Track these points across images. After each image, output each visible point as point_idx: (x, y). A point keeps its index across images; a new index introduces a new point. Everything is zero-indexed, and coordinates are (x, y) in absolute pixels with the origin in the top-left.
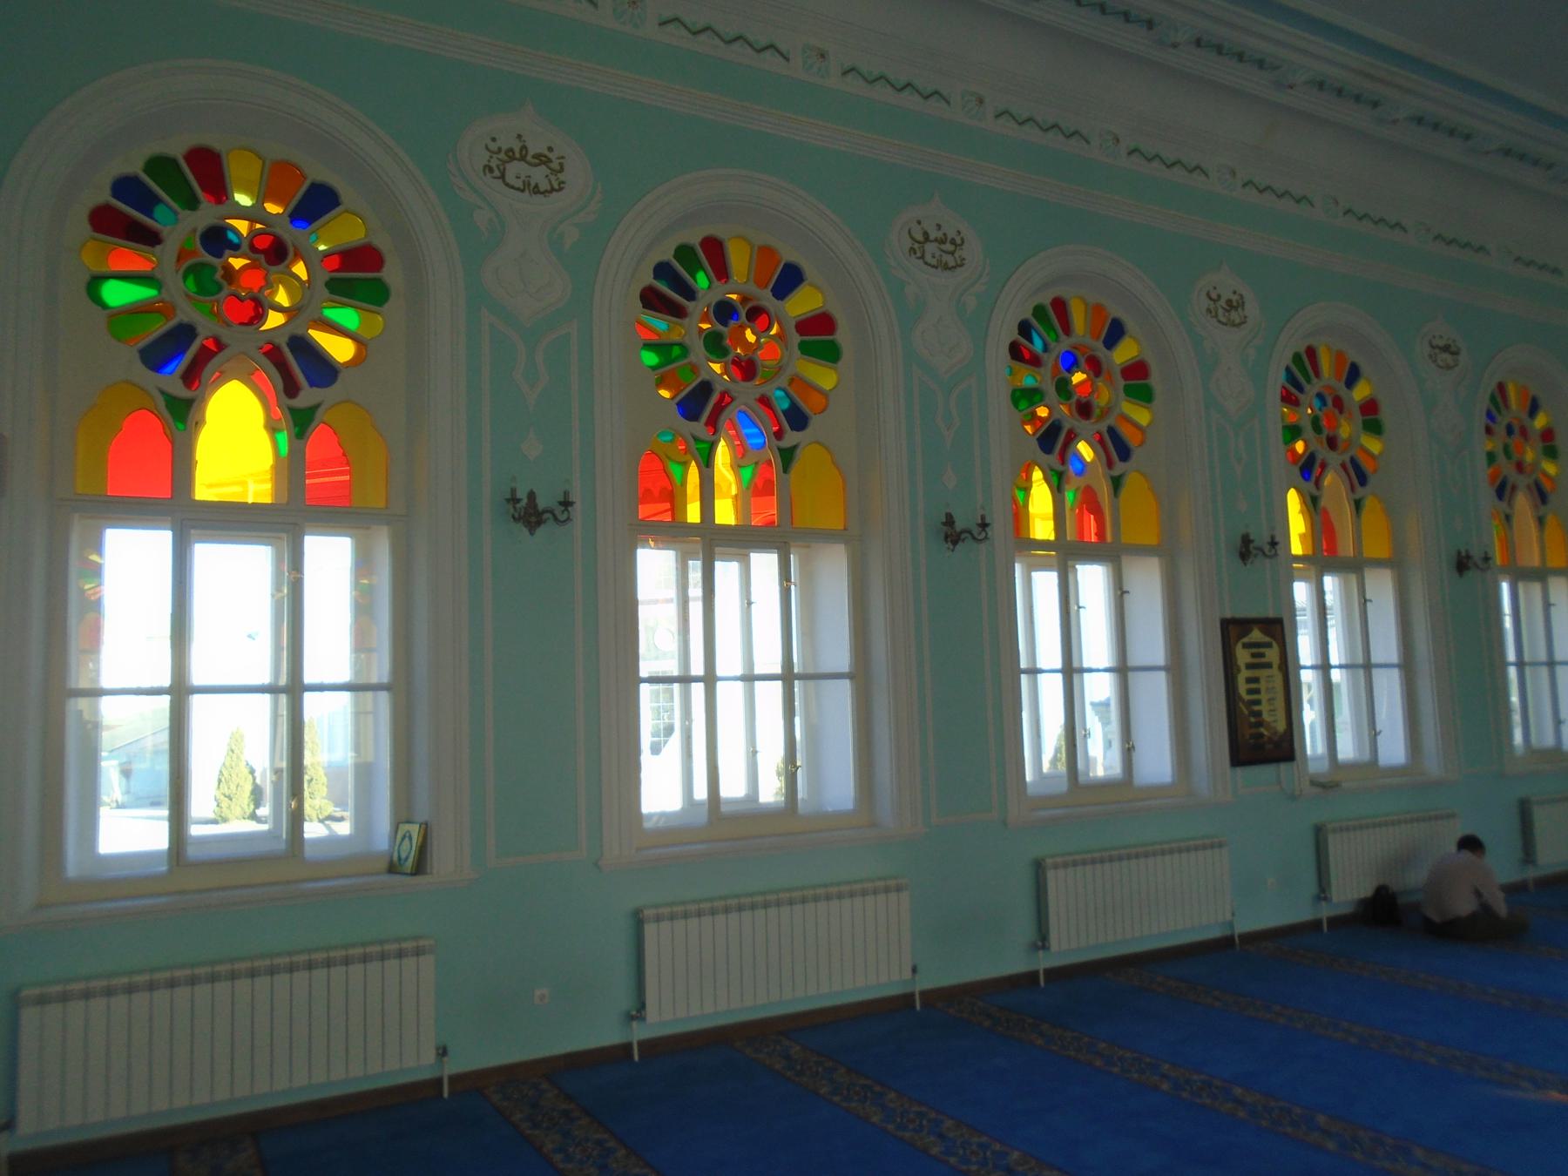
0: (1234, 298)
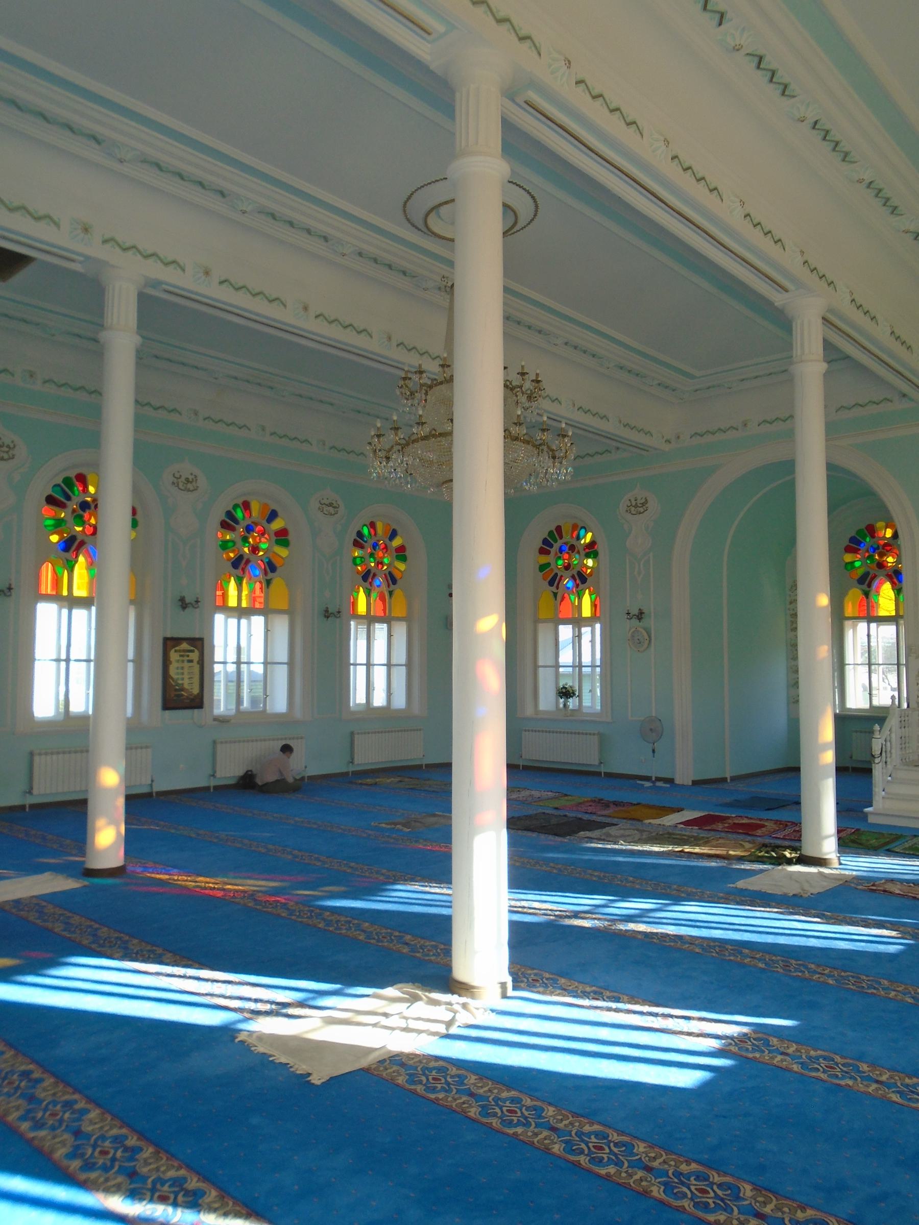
0: (190, 478)
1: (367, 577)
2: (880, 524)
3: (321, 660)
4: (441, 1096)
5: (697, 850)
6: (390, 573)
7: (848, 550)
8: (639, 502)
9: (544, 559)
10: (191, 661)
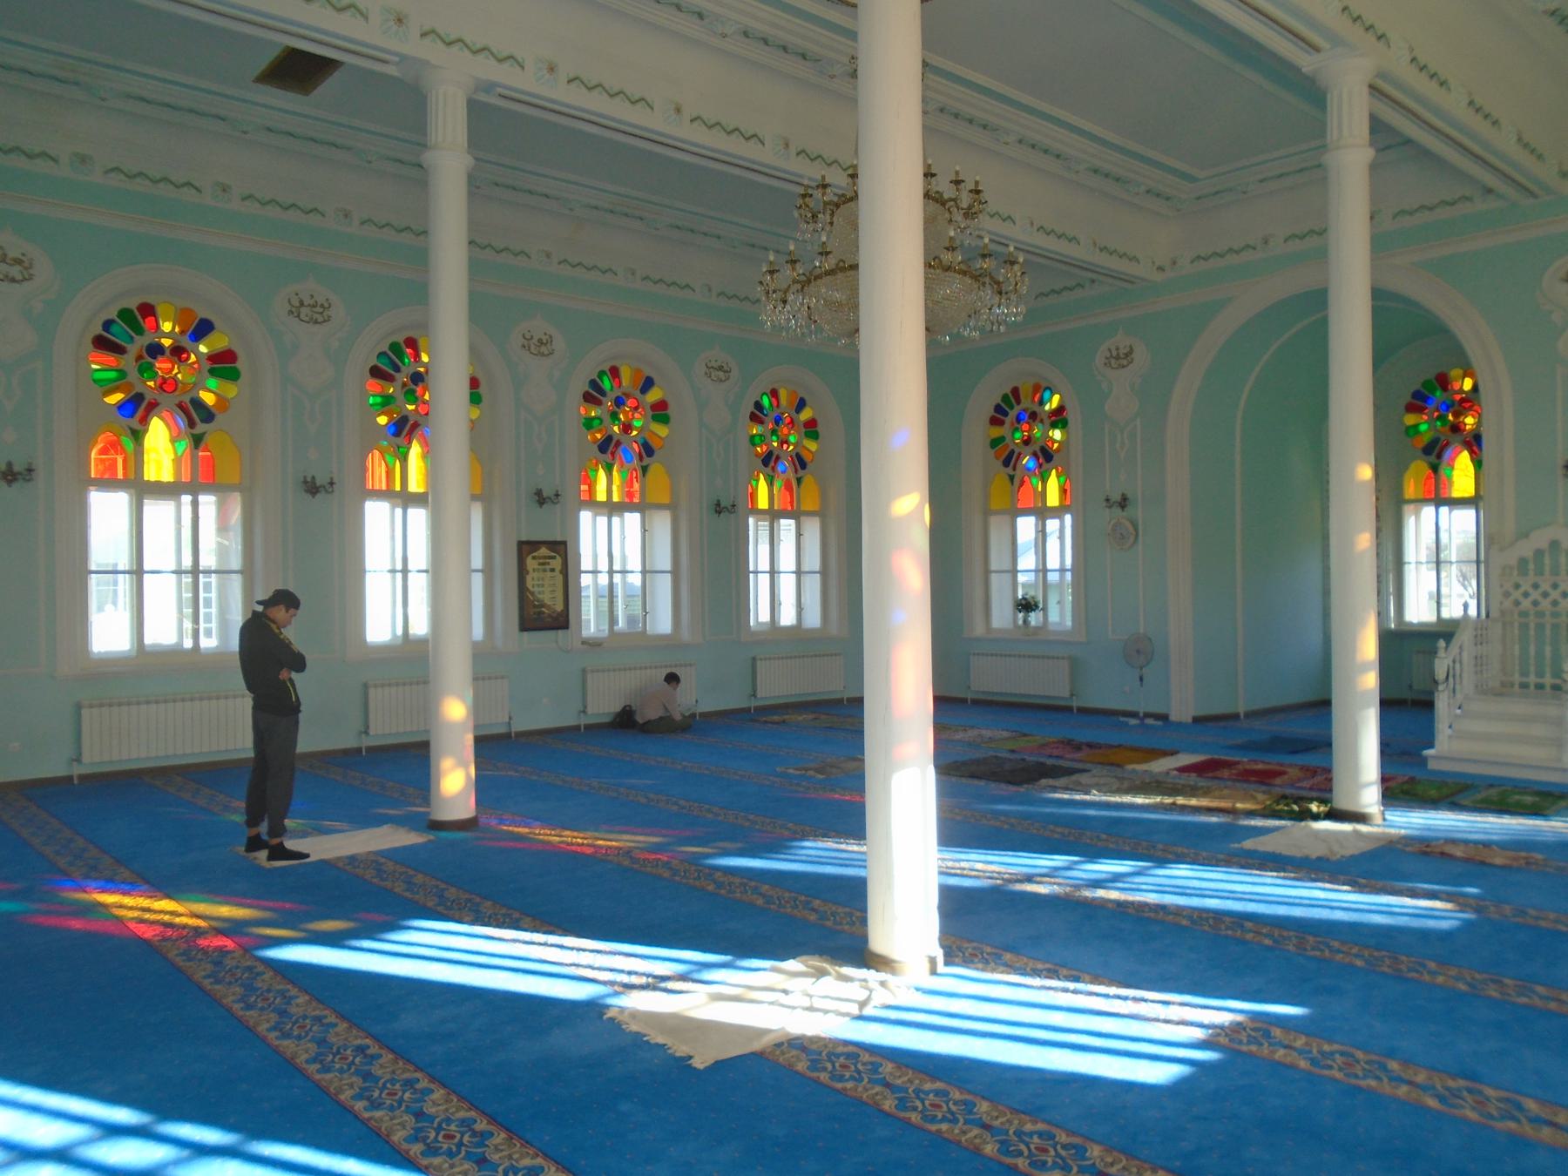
0: (544, 339)
1: (769, 460)
2: (1455, 373)
3: (713, 570)
4: (849, 1085)
5: (1193, 802)
6: (798, 455)
7: (1411, 408)
8: (1122, 351)
9: (996, 432)
10: (553, 570)
